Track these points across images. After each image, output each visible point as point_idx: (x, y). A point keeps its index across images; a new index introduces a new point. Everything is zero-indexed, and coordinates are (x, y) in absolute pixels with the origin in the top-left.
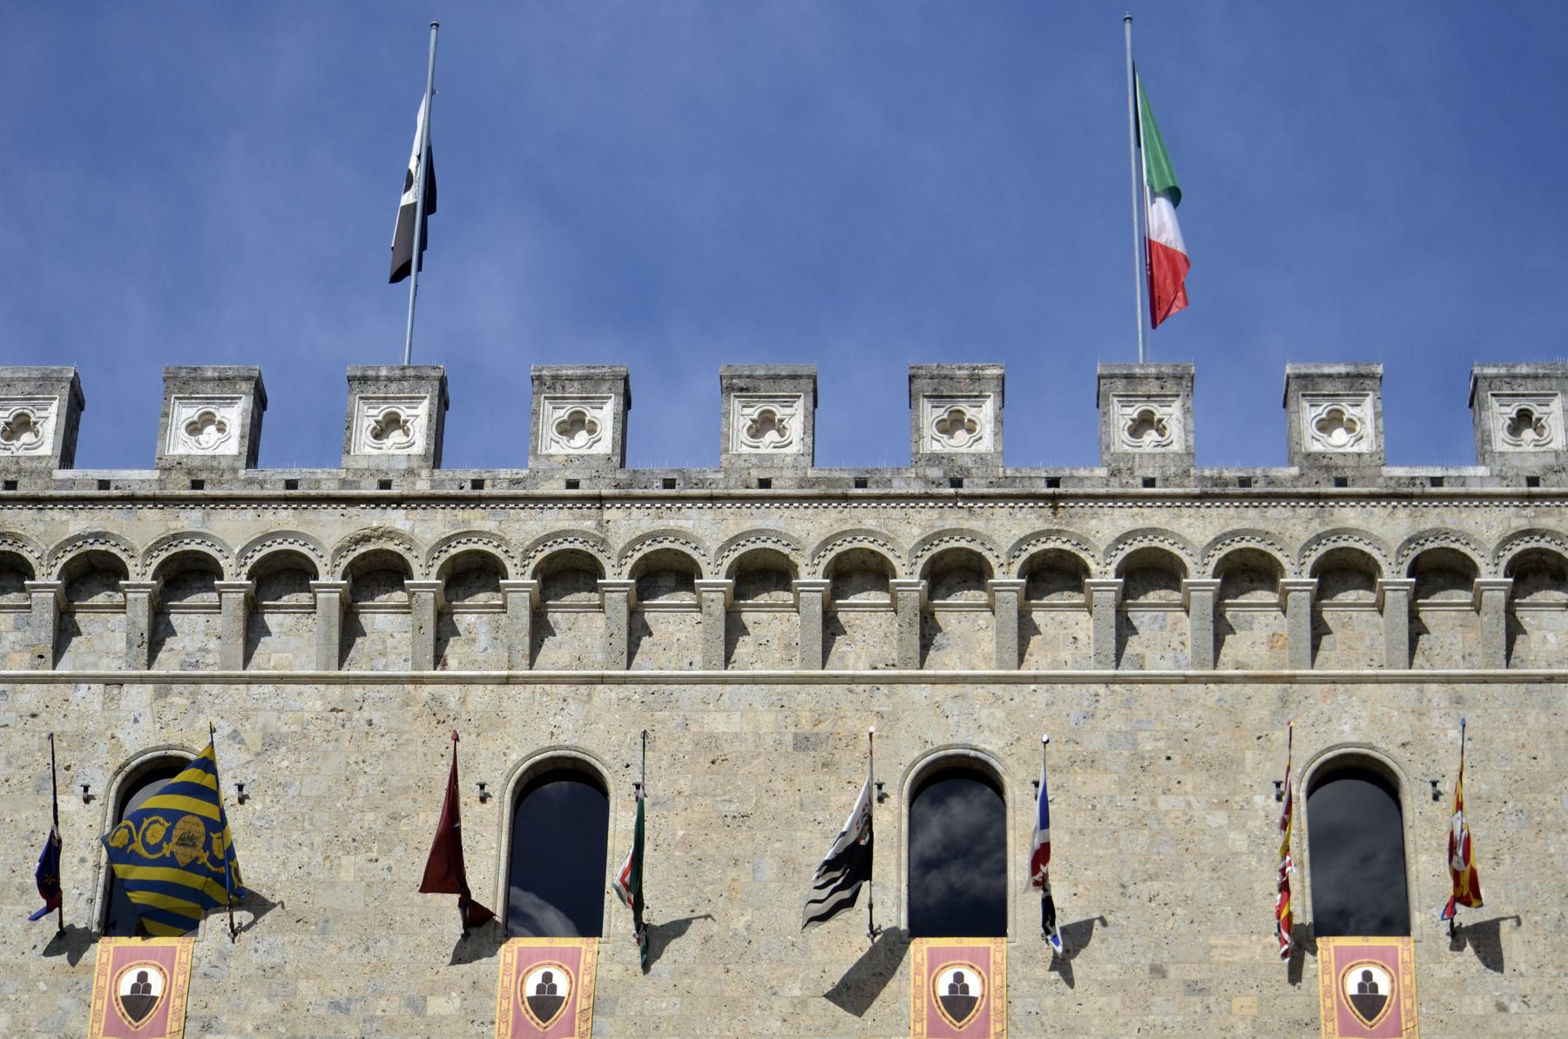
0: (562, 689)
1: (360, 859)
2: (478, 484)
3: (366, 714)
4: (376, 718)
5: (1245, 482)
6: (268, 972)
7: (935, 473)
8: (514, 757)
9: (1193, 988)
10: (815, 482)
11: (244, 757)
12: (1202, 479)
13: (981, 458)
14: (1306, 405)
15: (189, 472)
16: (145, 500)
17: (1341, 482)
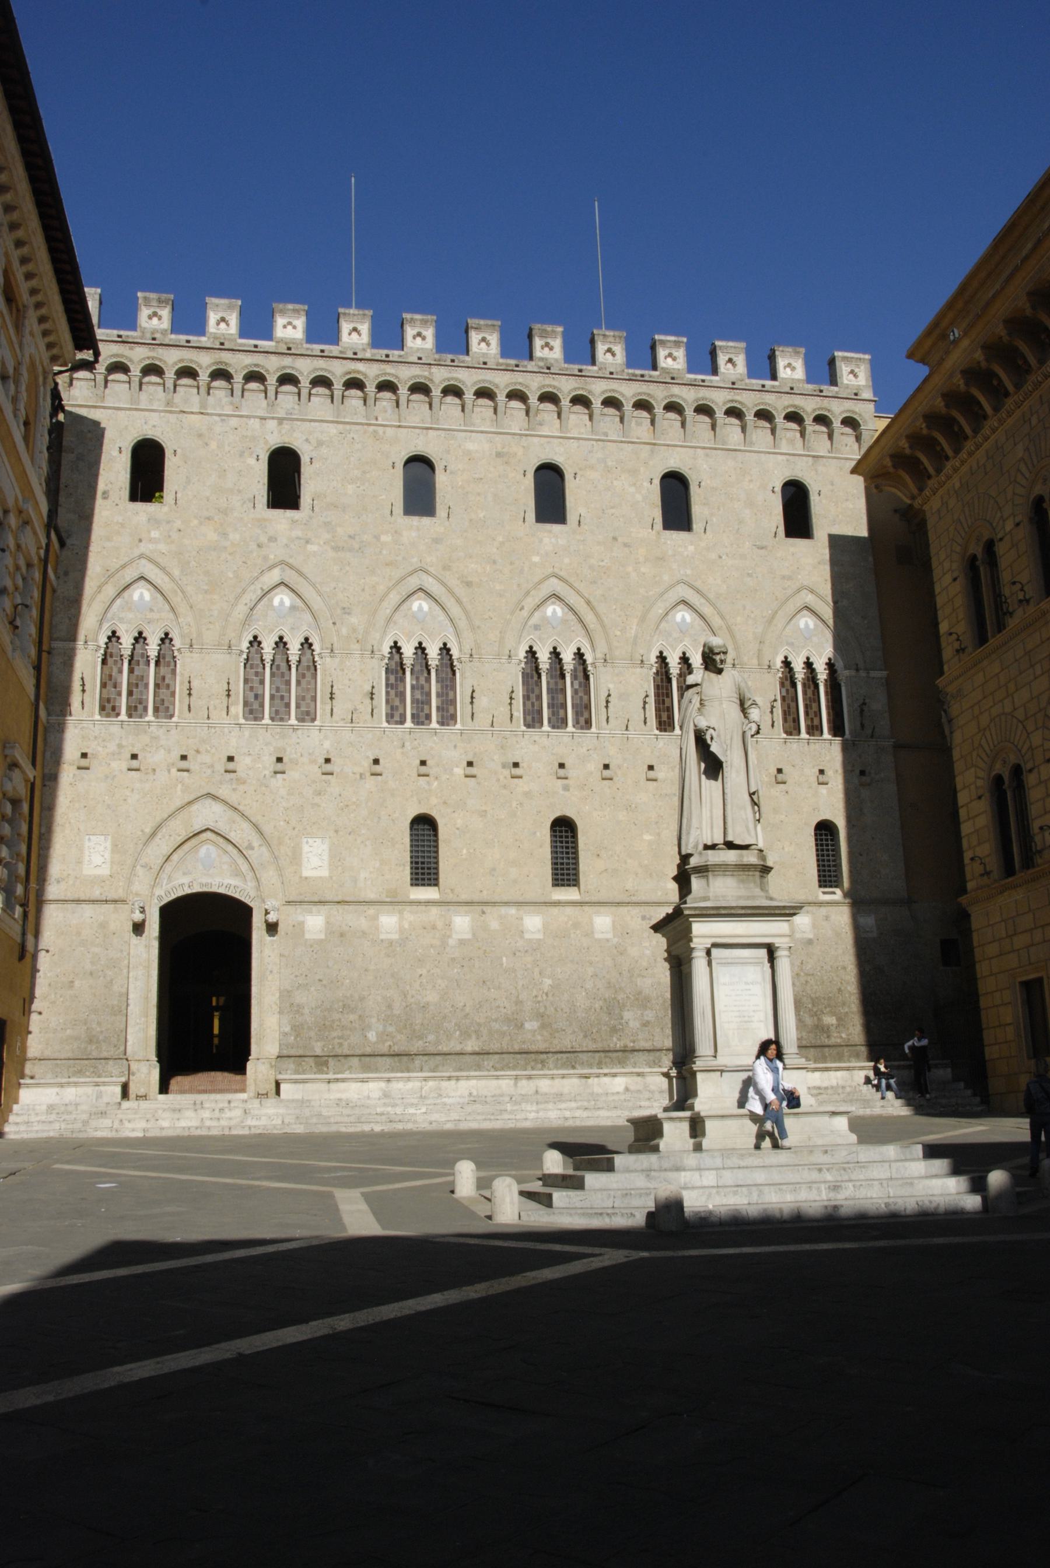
0: (418, 431)
2: (387, 356)
3: (352, 435)
4: (355, 437)
5: (642, 376)
6: (327, 524)
7: (541, 364)
9: (626, 545)
10: (501, 365)
12: (628, 374)
13: (556, 360)
15: (286, 343)
16: (272, 353)
17: (673, 378)
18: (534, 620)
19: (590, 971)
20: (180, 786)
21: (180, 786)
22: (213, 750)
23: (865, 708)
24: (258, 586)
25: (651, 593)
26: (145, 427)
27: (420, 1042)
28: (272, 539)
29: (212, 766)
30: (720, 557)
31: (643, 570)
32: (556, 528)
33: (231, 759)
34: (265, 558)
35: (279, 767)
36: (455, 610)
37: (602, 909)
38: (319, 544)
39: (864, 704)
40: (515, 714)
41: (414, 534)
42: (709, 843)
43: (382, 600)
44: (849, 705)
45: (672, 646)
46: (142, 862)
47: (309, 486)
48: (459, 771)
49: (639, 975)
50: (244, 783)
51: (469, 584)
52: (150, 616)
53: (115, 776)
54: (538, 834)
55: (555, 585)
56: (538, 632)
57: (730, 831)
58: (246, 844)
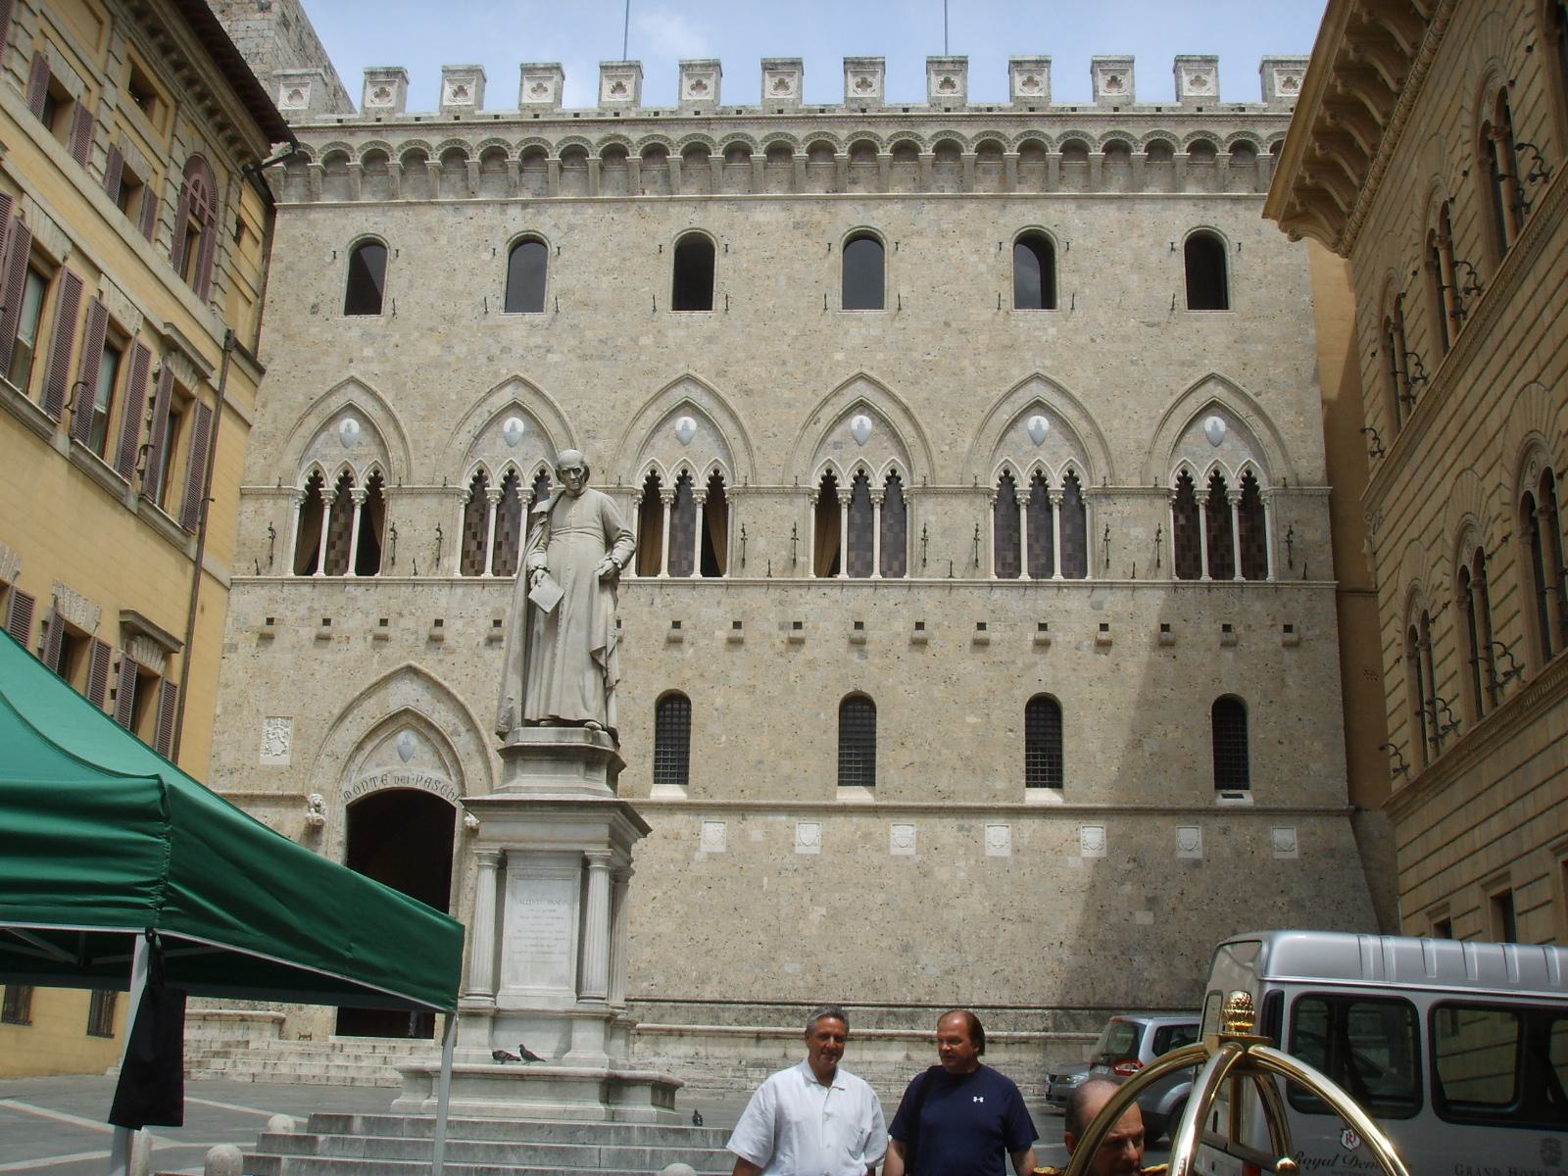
1: (610, 278)
4: (615, 216)
8: (674, 233)
9: (962, 332)
11: (560, 234)
14: (1016, 74)
15: (533, 110)
17: (1032, 109)
18: (836, 436)
19: (880, 897)
20: (376, 657)
21: (376, 657)
22: (419, 613)
23: (1295, 539)
24: (485, 408)
25: (992, 394)
26: (366, 224)
27: (645, 984)
28: (505, 350)
29: (416, 632)
30: (1093, 340)
31: (984, 363)
32: (868, 314)
33: (439, 623)
34: (496, 374)
35: (496, 631)
36: (728, 429)
37: (904, 820)
38: (562, 352)
39: (1291, 532)
40: (801, 559)
41: (682, 333)
42: (534, 719)
43: (636, 419)
44: (1273, 535)
45: (1020, 462)
46: (328, 750)
47: (557, 282)
48: (723, 634)
49: (947, 905)
50: (454, 652)
51: (748, 393)
52: (358, 451)
53: (303, 646)
54: (822, 716)
55: (861, 390)
56: (838, 451)
57: (554, 701)
58: (451, 729)
